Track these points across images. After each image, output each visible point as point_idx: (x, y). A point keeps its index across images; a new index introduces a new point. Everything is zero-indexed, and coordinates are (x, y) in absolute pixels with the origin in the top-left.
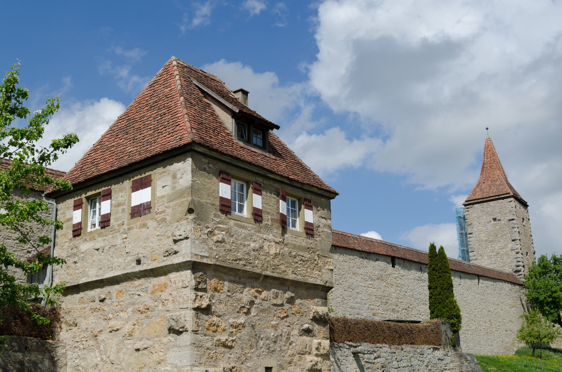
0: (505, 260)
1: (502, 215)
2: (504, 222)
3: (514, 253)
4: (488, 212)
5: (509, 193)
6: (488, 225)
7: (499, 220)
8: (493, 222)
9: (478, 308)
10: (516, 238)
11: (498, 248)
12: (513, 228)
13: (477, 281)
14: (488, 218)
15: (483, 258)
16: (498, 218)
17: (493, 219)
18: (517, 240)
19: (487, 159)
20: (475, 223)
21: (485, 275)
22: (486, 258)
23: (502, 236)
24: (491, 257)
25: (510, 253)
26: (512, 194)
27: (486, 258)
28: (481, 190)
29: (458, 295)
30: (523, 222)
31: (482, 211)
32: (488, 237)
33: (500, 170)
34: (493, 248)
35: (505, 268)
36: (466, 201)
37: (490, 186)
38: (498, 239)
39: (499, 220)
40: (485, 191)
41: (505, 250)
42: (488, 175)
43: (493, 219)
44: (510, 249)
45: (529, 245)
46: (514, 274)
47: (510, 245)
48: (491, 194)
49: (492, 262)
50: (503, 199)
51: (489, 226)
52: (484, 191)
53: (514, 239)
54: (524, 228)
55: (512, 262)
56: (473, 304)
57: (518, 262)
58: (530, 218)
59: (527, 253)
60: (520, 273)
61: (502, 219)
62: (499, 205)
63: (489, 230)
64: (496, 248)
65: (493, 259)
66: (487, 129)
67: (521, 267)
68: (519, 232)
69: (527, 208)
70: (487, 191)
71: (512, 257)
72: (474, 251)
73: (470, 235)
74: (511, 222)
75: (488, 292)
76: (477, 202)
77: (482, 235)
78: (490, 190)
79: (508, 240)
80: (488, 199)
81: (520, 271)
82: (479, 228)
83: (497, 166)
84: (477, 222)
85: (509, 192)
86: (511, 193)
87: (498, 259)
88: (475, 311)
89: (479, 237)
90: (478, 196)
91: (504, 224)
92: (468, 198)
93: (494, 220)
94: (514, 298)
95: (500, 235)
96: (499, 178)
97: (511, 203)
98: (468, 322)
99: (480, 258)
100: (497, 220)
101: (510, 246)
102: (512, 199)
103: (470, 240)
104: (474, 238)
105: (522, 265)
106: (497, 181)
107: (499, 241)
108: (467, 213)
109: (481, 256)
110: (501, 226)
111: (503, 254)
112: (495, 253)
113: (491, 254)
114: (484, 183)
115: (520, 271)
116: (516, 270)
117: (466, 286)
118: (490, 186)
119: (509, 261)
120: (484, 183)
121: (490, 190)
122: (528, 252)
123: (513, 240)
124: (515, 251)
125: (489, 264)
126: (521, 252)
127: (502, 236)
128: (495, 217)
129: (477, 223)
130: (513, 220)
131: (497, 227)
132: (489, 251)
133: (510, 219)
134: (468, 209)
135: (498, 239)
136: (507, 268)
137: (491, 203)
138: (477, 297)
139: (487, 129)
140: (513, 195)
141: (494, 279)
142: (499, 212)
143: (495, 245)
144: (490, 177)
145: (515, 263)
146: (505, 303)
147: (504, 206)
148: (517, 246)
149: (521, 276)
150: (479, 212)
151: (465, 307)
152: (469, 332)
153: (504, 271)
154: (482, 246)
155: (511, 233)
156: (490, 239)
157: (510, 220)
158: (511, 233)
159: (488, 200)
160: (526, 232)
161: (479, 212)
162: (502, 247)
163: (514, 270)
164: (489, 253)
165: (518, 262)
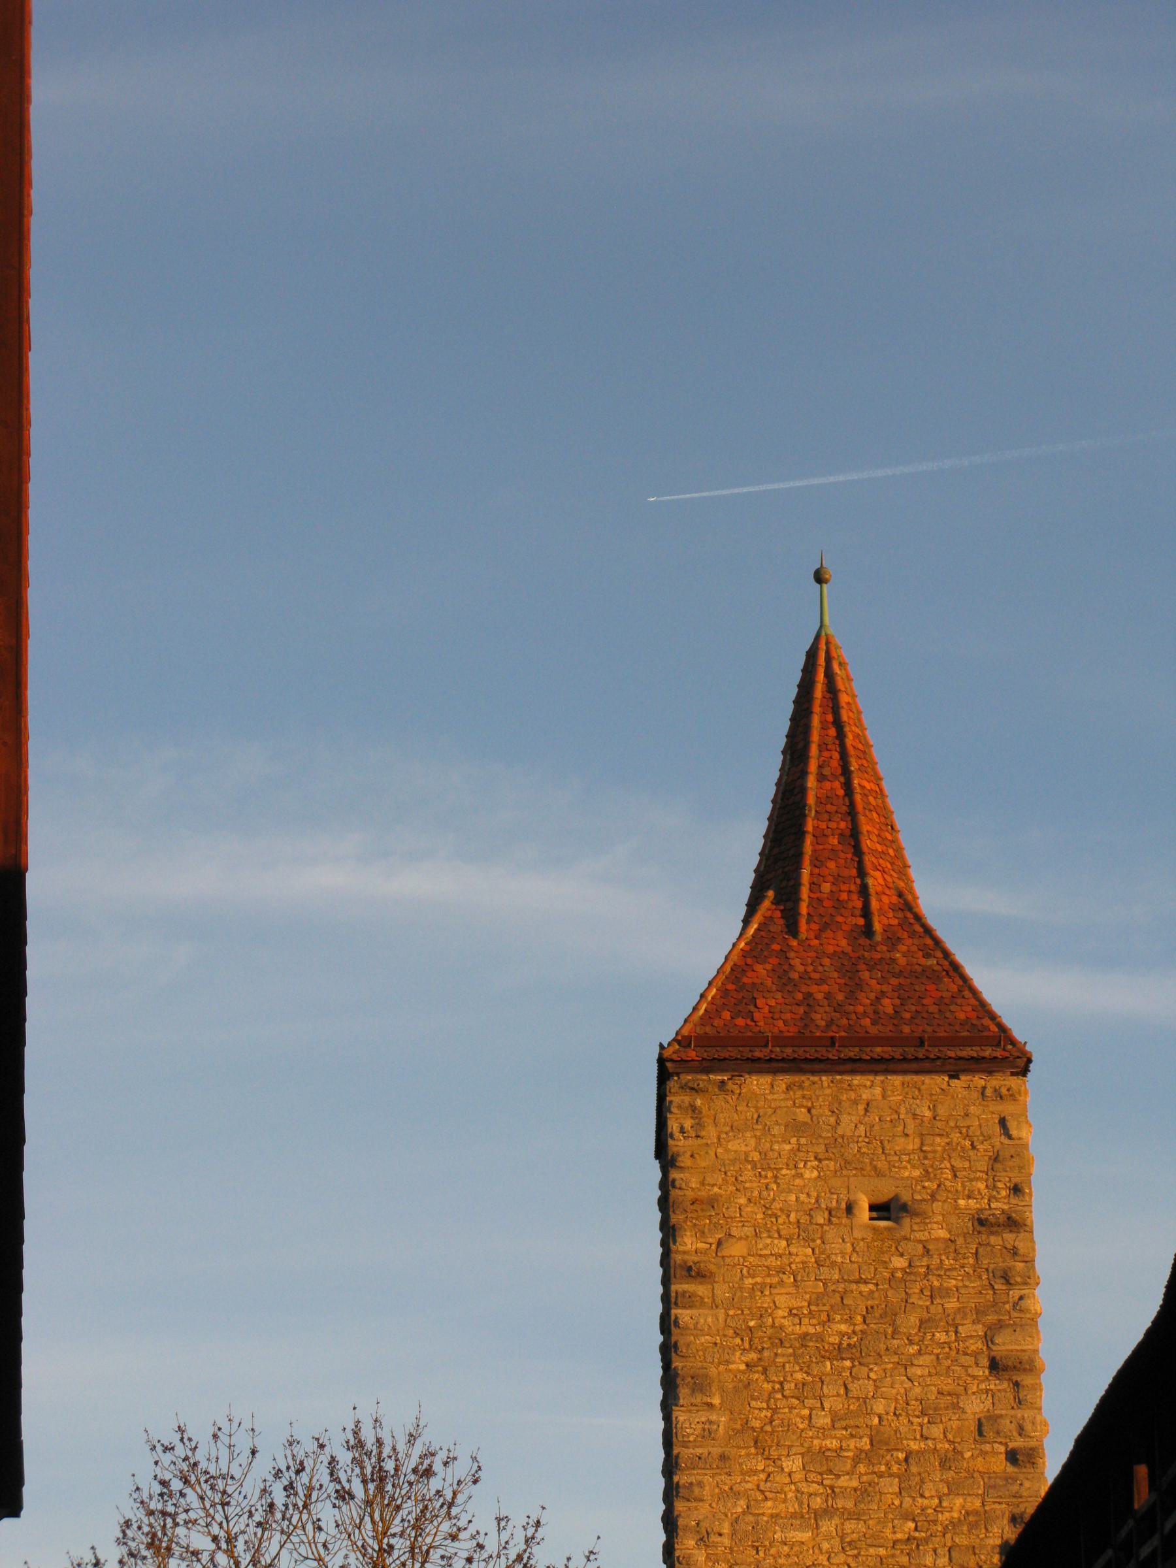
2: (943, 1234)
4: (836, 1143)
6: (831, 1233)
14: (836, 1182)
27: (793, 1464)
31: (797, 1128)
41: (936, 1431)
48: (867, 1022)
49: (840, 1503)
50: (954, 1076)
51: (838, 1247)
52: (809, 995)
70: (828, 996)
74: (993, 1240)
78: (851, 995)
95: (913, 1320)
101: (975, 1406)
111: (920, 1452)
112: (865, 1443)
121: (851, 995)
125: (818, 1515)
131: (899, 1263)
132: (823, 1420)
156: (835, 1339)
164: (824, 1432)
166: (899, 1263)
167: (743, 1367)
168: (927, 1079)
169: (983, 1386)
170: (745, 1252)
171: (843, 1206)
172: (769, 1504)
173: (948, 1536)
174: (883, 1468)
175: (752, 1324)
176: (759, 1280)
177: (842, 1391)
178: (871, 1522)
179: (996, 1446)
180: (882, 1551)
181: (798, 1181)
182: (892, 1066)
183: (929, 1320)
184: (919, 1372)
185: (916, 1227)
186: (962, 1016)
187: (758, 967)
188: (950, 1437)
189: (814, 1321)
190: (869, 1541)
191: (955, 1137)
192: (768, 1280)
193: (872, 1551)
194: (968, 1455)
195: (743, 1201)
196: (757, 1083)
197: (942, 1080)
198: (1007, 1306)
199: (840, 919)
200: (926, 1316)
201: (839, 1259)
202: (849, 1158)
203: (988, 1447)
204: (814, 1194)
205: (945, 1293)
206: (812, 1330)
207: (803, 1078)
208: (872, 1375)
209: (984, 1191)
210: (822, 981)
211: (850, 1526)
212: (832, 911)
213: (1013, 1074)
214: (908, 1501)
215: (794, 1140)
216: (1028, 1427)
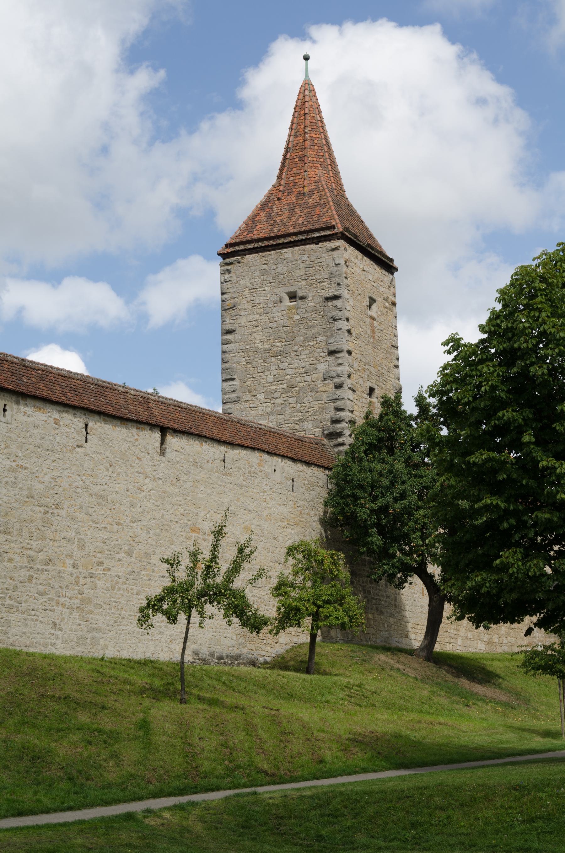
0: (308, 405)
1: (311, 285)
2: (313, 304)
3: (330, 385)
4: (278, 275)
5: (333, 227)
6: (274, 310)
7: (302, 298)
8: (287, 302)
9: (148, 517)
10: (339, 347)
11: (294, 371)
12: (335, 320)
13: (158, 444)
14: (276, 290)
15: (253, 398)
16: (300, 294)
17: (288, 293)
18: (341, 351)
19: (296, 136)
20: (243, 304)
21: (193, 431)
22: (261, 397)
23: (306, 340)
24: (276, 395)
25: (320, 386)
26: (340, 228)
27: (261, 397)
28: (269, 216)
29: (66, 473)
30: (370, 306)
31: (264, 272)
32: (271, 341)
33: (325, 168)
34: (282, 373)
35: (305, 425)
36: (227, 246)
37: (292, 212)
38: (296, 348)
39: (302, 298)
40: (278, 219)
41: (308, 378)
42: (291, 179)
43: (288, 293)
44: (321, 375)
45: (384, 371)
46: (325, 441)
47: (322, 365)
49: (276, 409)
50: (317, 244)
51: (276, 314)
52: (275, 221)
53: (332, 348)
54: (372, 325)
55: (323, 410)
56: (128, 504)
57: (338, 409)
58: (397, 300)
59: (372, 390)
60: (340, 440)
61: (310, 294)
62: (305, 258)
63: (275, 324)
64: (289, 371)
65: (279, 401)
66: (306, 58)
67: (343, 425)
68: (349, 331)
69: (392, 274)
71: (325, 397)
72: (233, 379)
73: (229, 337)
74: (330, 304)
75: (199, 478)
76: (253, 248)
77: (259, 336)
78: (289, 218)
79: (318, 350)
80: (281, 241)
81: (340, 434)
82: (251, 318)
83: (317, 156)
84: (248, 301)
85: (334, 223)
86: (339, 225)
87: (292, 400)
88: (134, 525)
89: (250, 342)
90: (260, 231)
91: (315, 310)
92: (232, 238)
93: (290, 299)
94: (301, 503)
96: (317, 188)
97: (335, 253)
98: (99, 555)
99: (247, 397)
100: (298, 298)
101: (322, 367)
102: (340, 243)
103: (227, 350)
104: (237, 345)
105: (347, 420)
106: (311, 193)
107: (298, 353)
108: (227, 276)
109: (249, 391)
110: (306, 315)
111: (303, 387)
113: (274, 387)
114: (279, 199)
115: (340, 434)
116: (331, 430)
117: (108, 454)
118: (292, 212)
119: (316, 406)
120: (279, 199)
121: (289, 218)
122: (376, 387)
123: (331, 353)
124: (335, 380)
125: (269, 414)
126: (348, 383)
127: (306, 340)
128: (292, 289)
129: (249, 305)
130: (336, 297)
131: (297, 317)
132: (271, 379)
133: (331, 294)
134: (229, 267)
135: (296, 348)
136: (310, 426)
137: (288, 253)
138: (150, 486)
139: (306, 58)
140: (342, 233)
141: (205, 437)
142: (303, 277)
143: (286, 364)
144: (295, 184)
145: (330, 414)
146: (265, 514)
147: (319, 261)
148: (340, 368)
149: (342, 448)
150: (257, 274)
151: (91, 510)
152: (100, 583)
153: (302, 434)
154: (254, 364)
155: (328, 333)
156: (275, 349)
157: (328, 299)
158: (328, 333)
159: (280, 244)
160: (377, 334)
161: (257, 274)
162: (303, 370)
163: (326, 432)
165: (338, 409)
166: (297, 317)
167: (245, 363)
168: (307, 246)
169: (325, 359)
170: (245, 321)
171: (279, 299)
172: (253, 412)
173: (313, 417)
174: (291, 394)
175: (247, 347)
176: (250, 331)
177: (277, 368)
178: (286, 415)
179: (330, 381)
180: (290, 424)
181: (264, 292)
182: (295, 244)
183: (307, 338)
184: (303, 357)
185: (302, 303)
186: (325, 220)
187: (262, 213)
188: (314, 380)
189: (268, 343)
190: (286, 422)
191: (317, 268)
192: (253, 330)
193: (287, 425)
194: (319, 386)
195: (245, 302)
196: (250, 258)
197: (313, 246)
198: (334, 328)
199: (294, 190)
200: (306, 336)
201: (277, 319)
202: (280, 280)
203: (326, 382)
204: (269, 296)
205: (312, 326)
206: (268, 347)
207: (265, 253)
208: (287, 361)
209: (327, 286)
210: (282, 215)
211: (279, 417)
212: (292, 187)
213: (338, 239)
214: (299, 405)
215: (262, 277)
216: (339, 372)
